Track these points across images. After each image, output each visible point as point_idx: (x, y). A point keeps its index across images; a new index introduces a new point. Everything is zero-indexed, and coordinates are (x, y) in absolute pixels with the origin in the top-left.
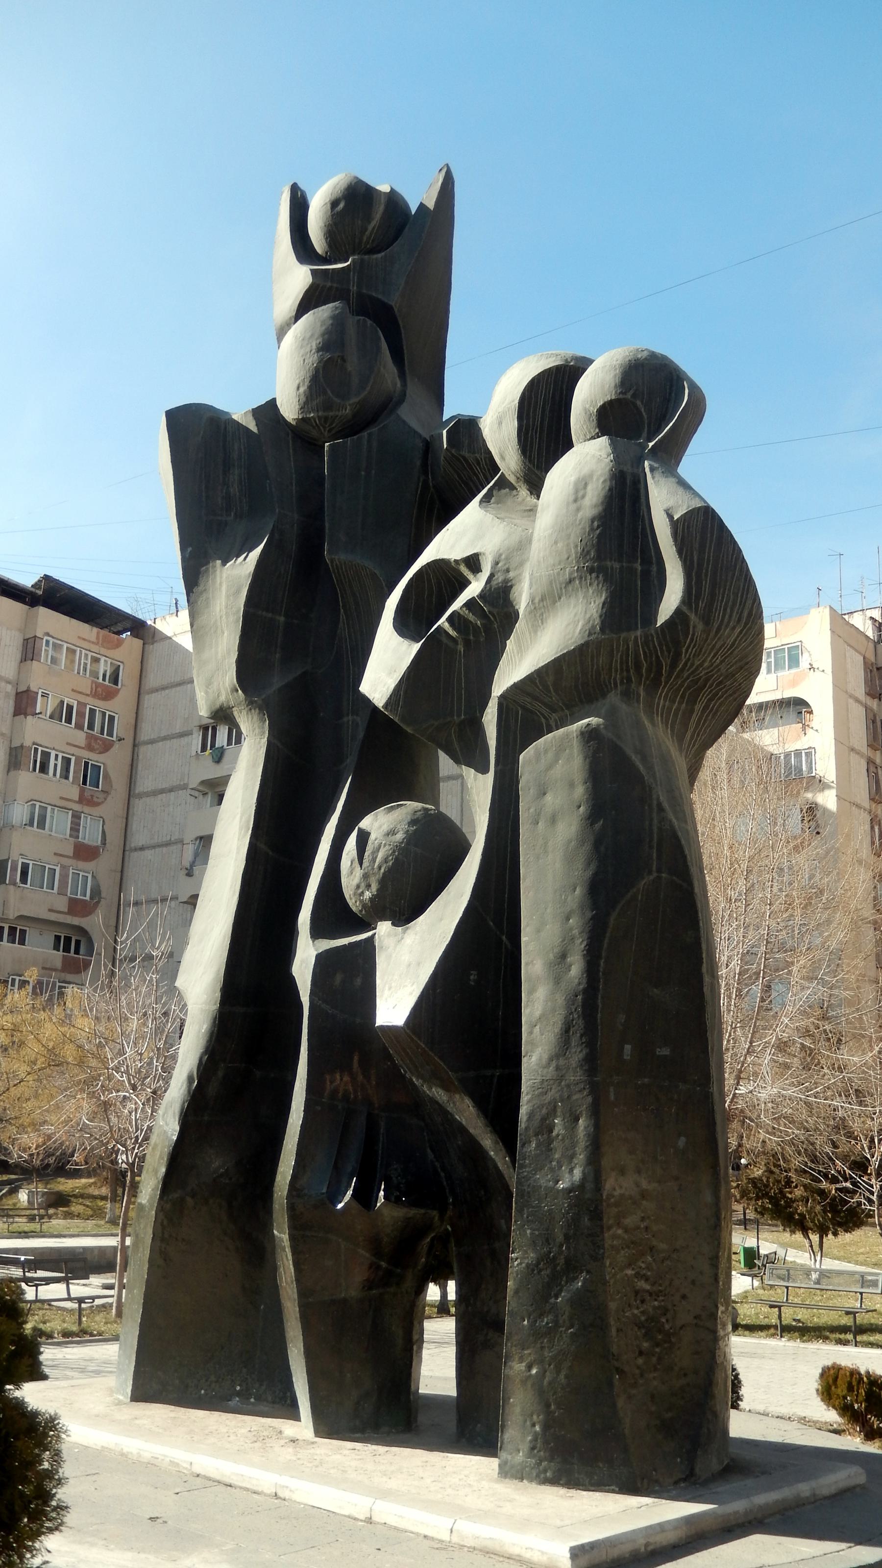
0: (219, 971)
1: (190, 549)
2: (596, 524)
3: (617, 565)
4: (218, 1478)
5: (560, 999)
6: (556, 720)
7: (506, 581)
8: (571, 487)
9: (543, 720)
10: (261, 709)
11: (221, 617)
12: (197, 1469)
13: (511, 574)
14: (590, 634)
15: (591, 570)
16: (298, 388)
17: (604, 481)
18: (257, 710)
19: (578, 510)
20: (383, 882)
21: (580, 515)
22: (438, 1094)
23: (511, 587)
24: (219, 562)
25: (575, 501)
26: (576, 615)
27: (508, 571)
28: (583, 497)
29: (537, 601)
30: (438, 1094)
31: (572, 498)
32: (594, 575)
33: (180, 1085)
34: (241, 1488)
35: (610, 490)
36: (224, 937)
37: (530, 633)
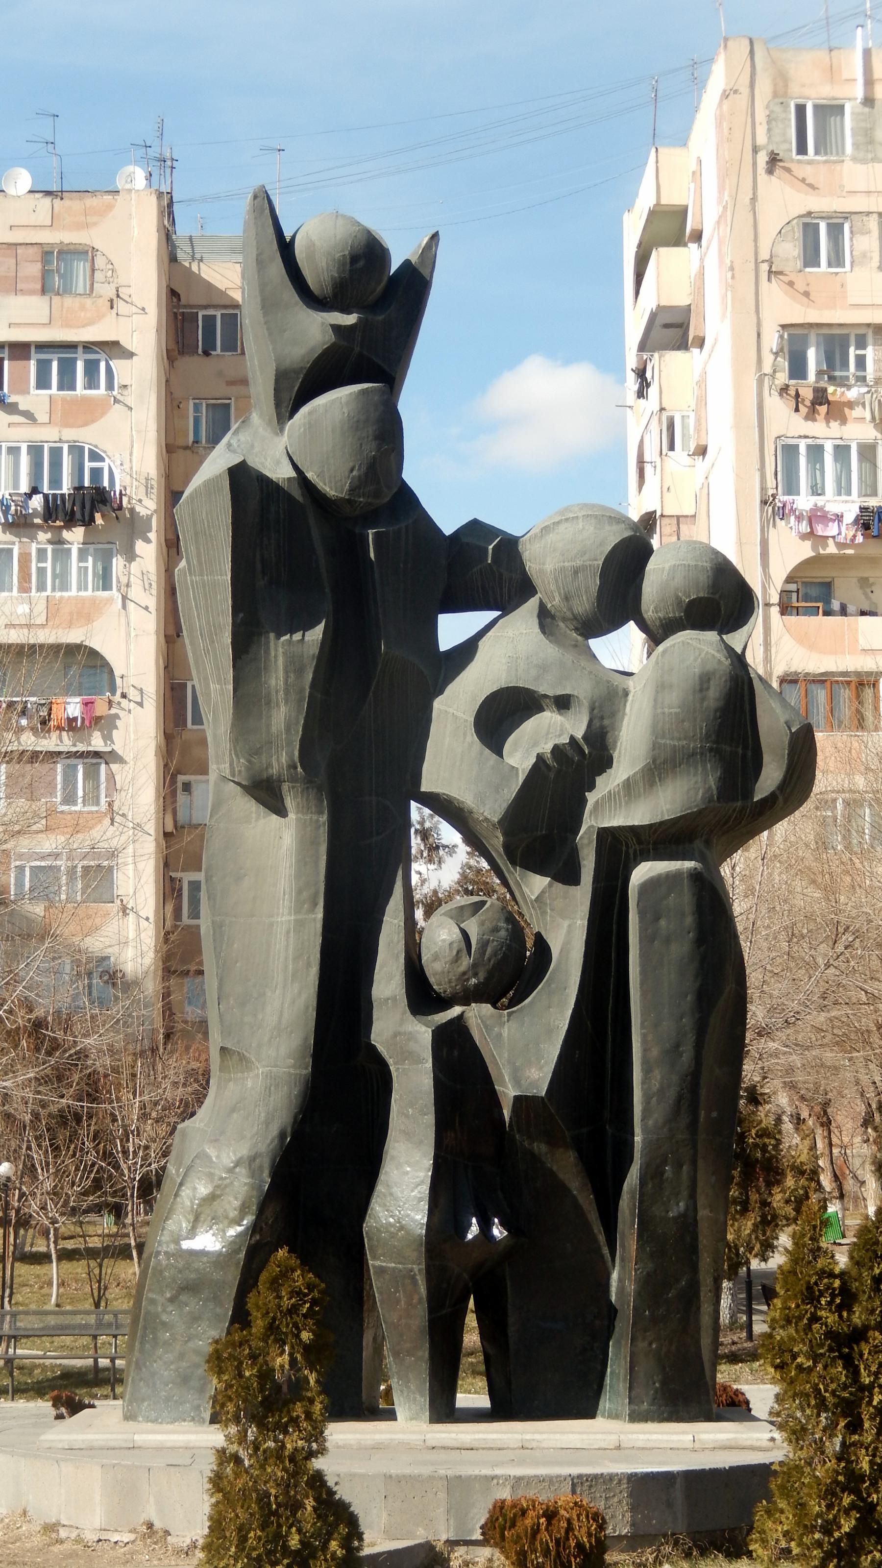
0: (306, 1039)
1: (241, 615)
2: (718, 714)
3: (728, 749)
4: (459, 1446)
5: (675, 1078)
6: (635, 851)
7: (602, 727)
8: (697, 678)
9: (624, 848)
10: (319, 790)
11: (277, 692)
12: (430, 1443)
13: (606, 722)
14: (709, 802)
15: (711, 750)
16: (352, 470)
17: (726, 681)
18: (315, 790)
19: (703, 699)
20: (490, 975)
21: (705, 704)
22: (540, 1148)
23: (607, 733)
24: (272, 635)
25: (701, 690)
26: (696, 782)
27: (602, 718)
28: (708, 689)
29: (658, 762)
30: (540, 1148)
31: (698, 688)
32: (713, 754)
33: (268, 1141)
34: (483, 1449)
35: (730, 689)
36: (307, 1008)
37: (644, 785)
